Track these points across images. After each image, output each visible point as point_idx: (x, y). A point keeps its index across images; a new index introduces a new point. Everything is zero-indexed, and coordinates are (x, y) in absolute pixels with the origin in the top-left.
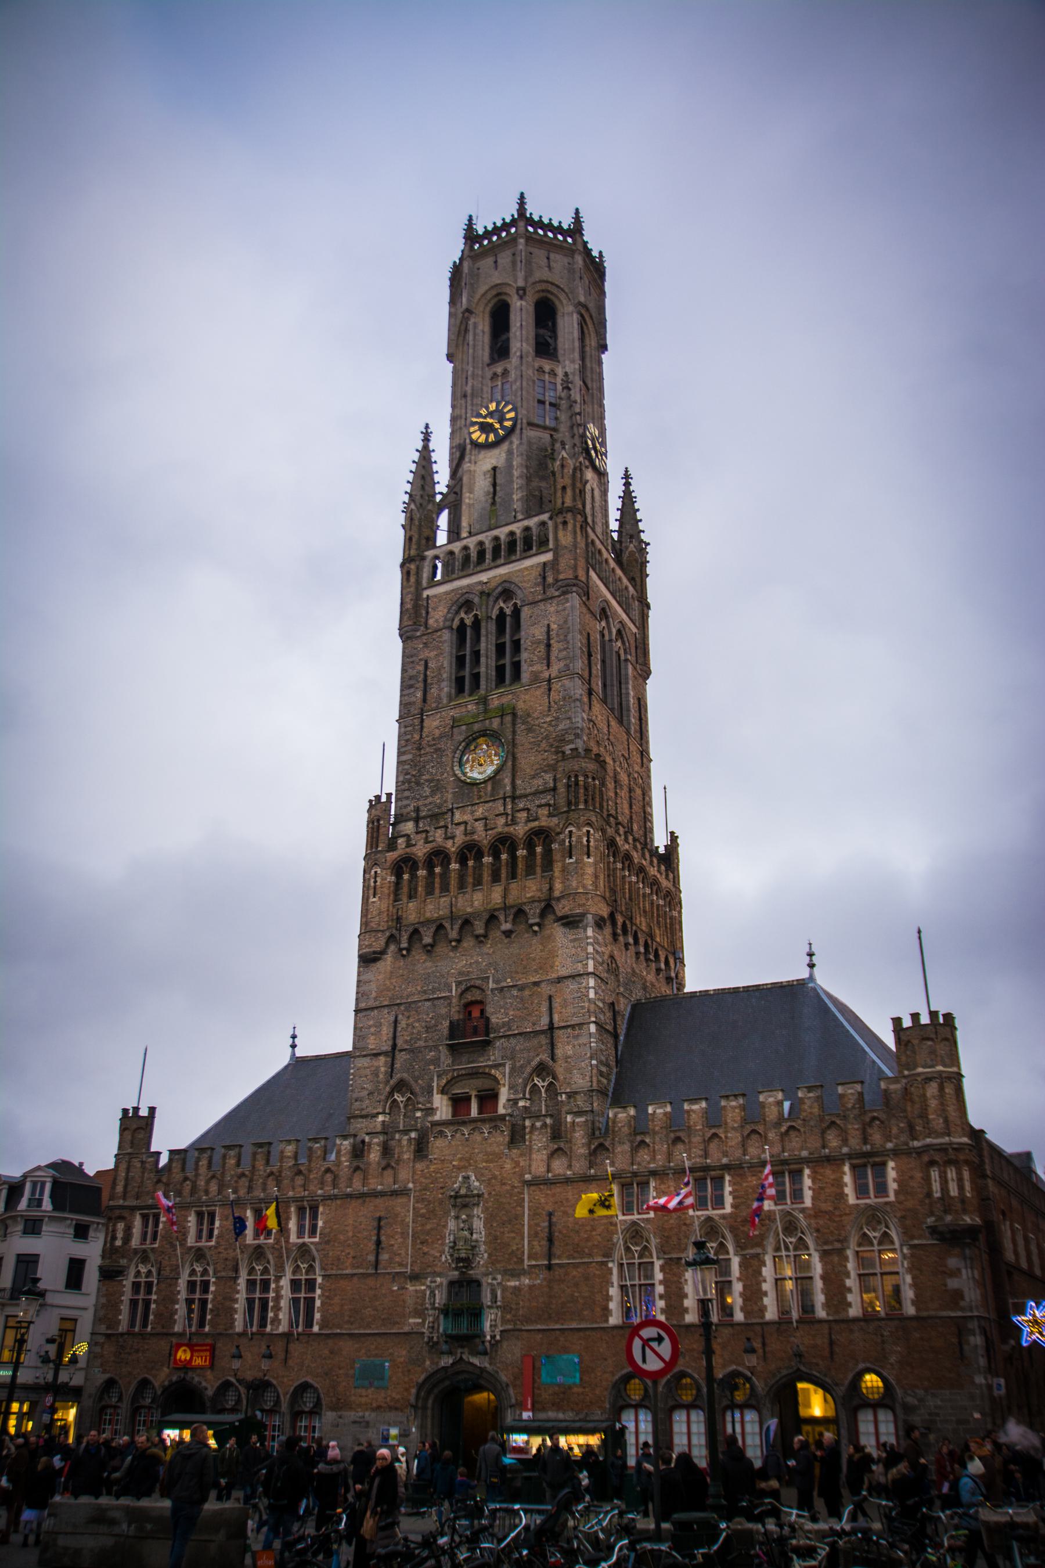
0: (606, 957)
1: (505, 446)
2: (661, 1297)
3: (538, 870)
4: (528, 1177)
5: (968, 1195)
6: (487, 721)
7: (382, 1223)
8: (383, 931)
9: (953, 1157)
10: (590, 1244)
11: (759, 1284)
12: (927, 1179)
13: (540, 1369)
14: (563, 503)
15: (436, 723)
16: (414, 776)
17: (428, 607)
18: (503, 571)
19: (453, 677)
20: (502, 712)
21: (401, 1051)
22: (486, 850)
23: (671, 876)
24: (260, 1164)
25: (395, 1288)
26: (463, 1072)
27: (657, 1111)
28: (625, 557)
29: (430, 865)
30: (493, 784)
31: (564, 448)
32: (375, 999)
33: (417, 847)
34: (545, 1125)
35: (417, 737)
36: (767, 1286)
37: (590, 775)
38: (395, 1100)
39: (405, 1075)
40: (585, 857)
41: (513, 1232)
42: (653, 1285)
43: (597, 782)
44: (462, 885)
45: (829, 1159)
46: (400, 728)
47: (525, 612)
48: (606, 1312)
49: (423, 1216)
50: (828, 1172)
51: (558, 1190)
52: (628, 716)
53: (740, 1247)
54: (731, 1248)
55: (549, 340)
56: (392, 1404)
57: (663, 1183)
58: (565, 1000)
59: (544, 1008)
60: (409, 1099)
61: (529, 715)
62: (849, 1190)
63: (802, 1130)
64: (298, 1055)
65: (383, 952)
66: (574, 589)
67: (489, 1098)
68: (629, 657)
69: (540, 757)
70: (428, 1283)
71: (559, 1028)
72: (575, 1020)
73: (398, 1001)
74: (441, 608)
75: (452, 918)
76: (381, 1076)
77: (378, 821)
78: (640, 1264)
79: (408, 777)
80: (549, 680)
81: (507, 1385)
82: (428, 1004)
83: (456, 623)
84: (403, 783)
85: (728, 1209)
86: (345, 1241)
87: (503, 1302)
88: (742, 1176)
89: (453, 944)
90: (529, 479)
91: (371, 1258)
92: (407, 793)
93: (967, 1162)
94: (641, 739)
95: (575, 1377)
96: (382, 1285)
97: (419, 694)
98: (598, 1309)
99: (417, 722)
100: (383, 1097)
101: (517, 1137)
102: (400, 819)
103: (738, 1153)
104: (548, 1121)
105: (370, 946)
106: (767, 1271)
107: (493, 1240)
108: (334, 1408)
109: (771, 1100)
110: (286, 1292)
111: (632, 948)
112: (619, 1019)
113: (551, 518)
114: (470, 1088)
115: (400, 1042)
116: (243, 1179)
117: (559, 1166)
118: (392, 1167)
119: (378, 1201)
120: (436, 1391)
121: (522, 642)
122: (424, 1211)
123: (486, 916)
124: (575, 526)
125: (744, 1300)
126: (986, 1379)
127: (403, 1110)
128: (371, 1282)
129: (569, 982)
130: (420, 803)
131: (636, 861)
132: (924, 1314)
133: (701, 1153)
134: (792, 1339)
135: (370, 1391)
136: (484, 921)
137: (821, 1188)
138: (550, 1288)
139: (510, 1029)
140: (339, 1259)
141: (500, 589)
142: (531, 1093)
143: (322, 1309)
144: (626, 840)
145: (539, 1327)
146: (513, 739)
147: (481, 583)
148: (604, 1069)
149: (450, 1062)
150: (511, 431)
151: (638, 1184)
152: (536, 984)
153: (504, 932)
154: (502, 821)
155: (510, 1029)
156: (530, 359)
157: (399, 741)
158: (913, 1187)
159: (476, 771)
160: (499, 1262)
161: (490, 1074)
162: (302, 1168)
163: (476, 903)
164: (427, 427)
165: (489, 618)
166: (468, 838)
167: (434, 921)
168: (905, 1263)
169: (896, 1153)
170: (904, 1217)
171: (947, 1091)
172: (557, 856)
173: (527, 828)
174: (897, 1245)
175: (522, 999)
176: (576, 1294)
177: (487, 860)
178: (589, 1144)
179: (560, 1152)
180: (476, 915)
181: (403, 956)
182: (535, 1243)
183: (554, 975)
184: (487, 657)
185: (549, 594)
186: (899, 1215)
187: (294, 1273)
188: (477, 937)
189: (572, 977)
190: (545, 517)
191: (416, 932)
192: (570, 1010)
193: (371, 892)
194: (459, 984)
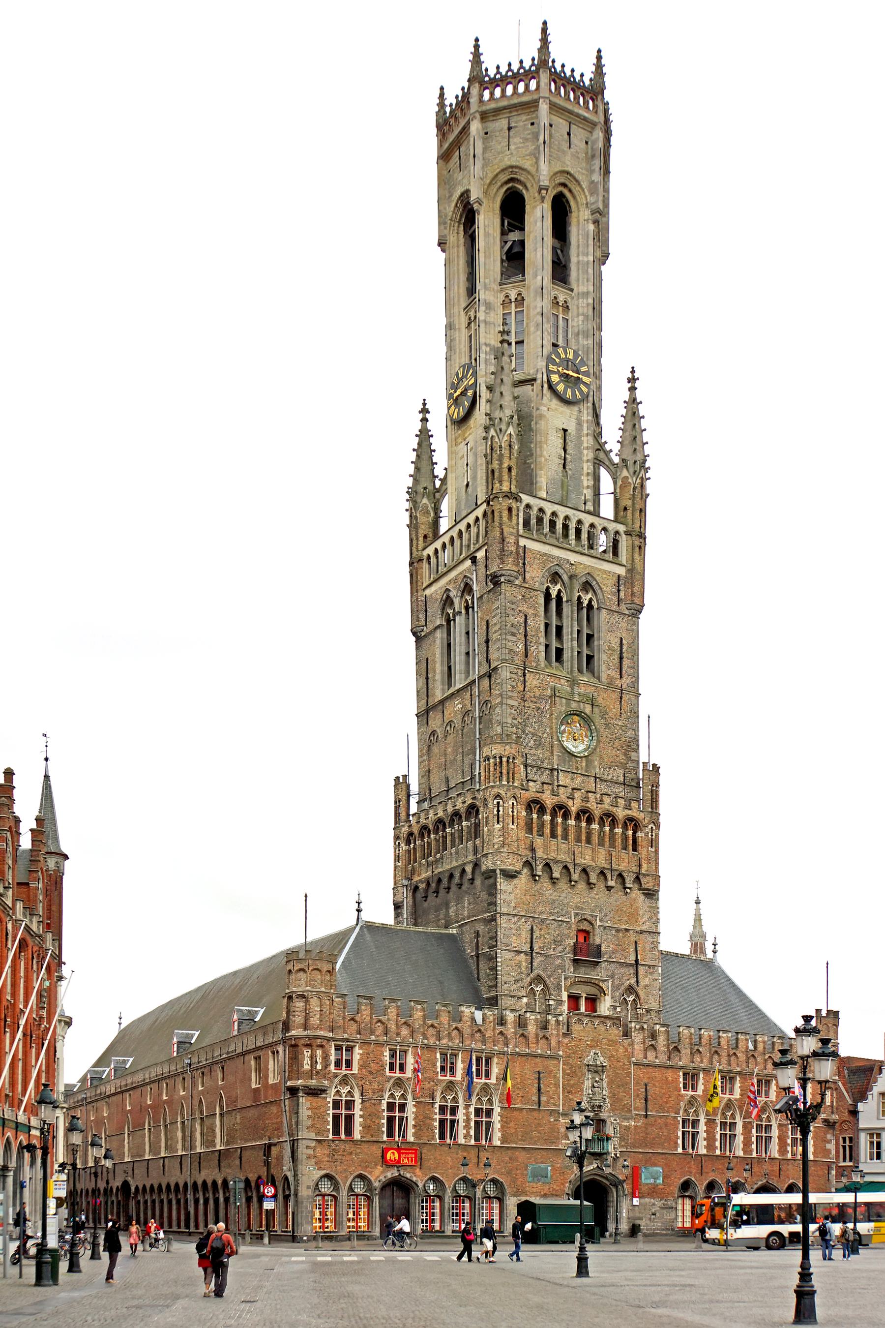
3: (630, 847)
7: (541, 1075)
8: (520, 855)
11: (751, 1137)
15: (536, 682)
24: (444, 1019)
29: (554, 815)
39: (541, 973)
44: (578, 840)
51: (650, 1070)
56: (554, 1192)
59: (632, 948)
60: (542, 989)
65: (519, 873)
67: (592, 1002)
73: (532, 915)
76: (523, 969)
77: (514, 758)
88: (745, 1079)
89: (573, 883)
91: (535, 1098)
97: (521, 647)
99: (520, 673)
100: (525, 985)
103: (744, 1065)
107: (613, 1096)
109: (761, 1039)
110: (472, 1116)
114: (583, 992)
115: (535, 947)
116: (431, 1029)
118: (547, 1039)
119: (538, 1060)
128: (535, 1114)
129: (647, 935)
132: (817, 1159)
133: (726, 1062)
138: (646, 1128)
143: (503, 1129)
145: (640, 1151)
152: (627, 930)
155: (610, 957)
160: (617, 1110)
161: (598, 985)
163: (587, 857)
166: (584, 804)
167: (562, 862)
175: (618, 937)
177: (595, 826)
181: (535, 880)
182: (637, 1101)
189: (650, 932)
194: (576, 915)
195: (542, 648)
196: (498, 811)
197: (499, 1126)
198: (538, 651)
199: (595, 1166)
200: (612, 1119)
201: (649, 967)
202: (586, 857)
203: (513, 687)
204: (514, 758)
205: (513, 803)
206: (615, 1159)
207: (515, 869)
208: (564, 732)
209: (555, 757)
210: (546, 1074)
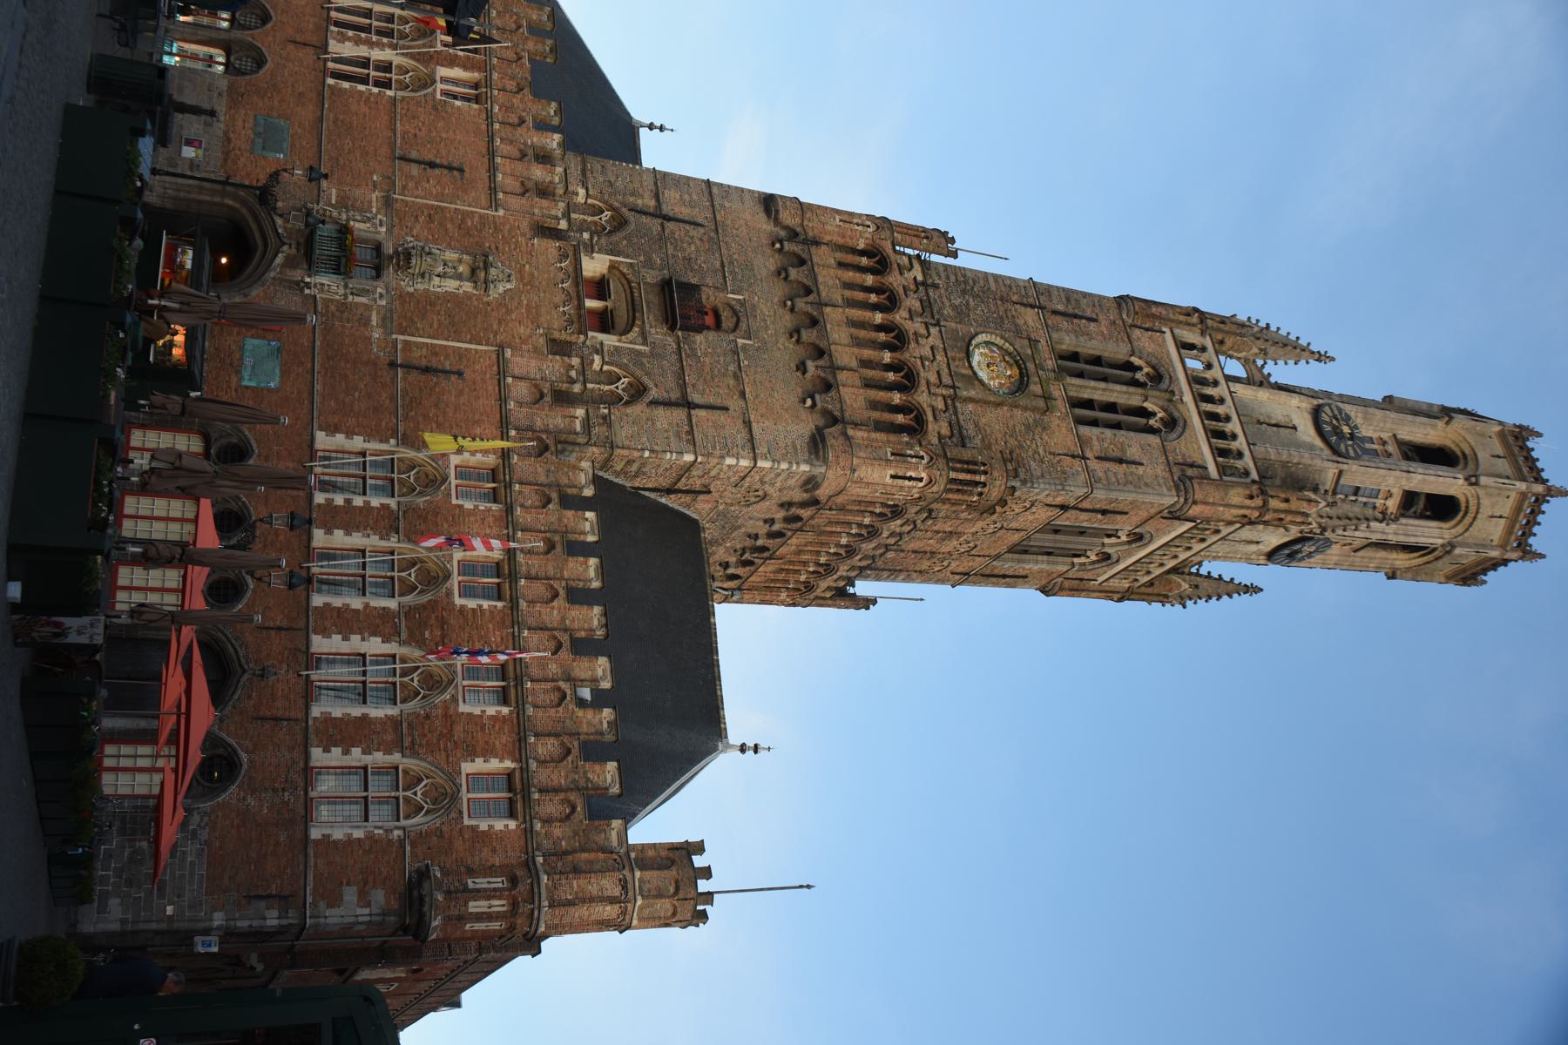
0: (767, 488)
1: (1318, 442)
2: (348, 501)
4: (508, 353)
5: (468, 927)
6: (1037, 379)
7: (455, 173)
9: (521, 911)
10: (420, 418)
12: (490, 871)
13: (264, 338)
14: (1272, 497)
15: (1030, 322)
16: (973, 288)
17: (1153, 330)
18: (1196, 420)
19: (1079, 350)
20: (1047, 397)
21: (662, 225)
22: (897, 355)
23: (828, 595)
24: (530, 45)
25: (375, 178)
26: (636, 294)
28: (1174, 577)
30: (968, 376)
31: (1328, 505)
32: (723, 206)
33: (899, 277)
34: (572, 382)
35: (1015, 298)
36: (356, 643)
37: (986, 490)
38: (603, 212)
39: (633, 227)
40: (892, 472)
41: (440, 325)
42: (364, 493)
43: (975, 498)
45: (521, 740)
46: (1024, 281)
47: (1154, 440)
48: (332, 430)
49: (463, 221)
50: (504, 739)
51: (490, 388)
52: (1013, 560)
53: (409, 612)
54: (408, 599)
55: (1413, 510)
56: (232, 156)
57: (496, 519)
58: (723, 427)
59: (712, 400)
61: (1044, 429)
62: (477, 765)
63: (560, 709)
64: (641, 129)
65: (777, 222)
66: (1182, 500)
67: (604, 322)
68: (1076, 568)
69: (999, 436)
70: (379, 217)
71: (689, 417)
72: (698, 436)
74: (1152, 345)
75: (821, 304)
76: (631, 199)
77: (927, 238)
78: (392, 480)
79: (971, 282)
80: (1084, 458)
81: (246, 296)
82: (718, 264)
83: (1135, 360)
84: (964, 276)
85: (458, 601)
86: (436, 129)
87: (351, 303)
89: (789, 303)
90: (1285, 464)
91: (414, 155)
92: (953, 278)
93: (512, 928)
94: (982, 575)
95: (250, 380)
96: (380, 163)
97: (1060, 307)
98: (336, 420)
99: (1031, 300)
100: (606, 197)
101: (560, 348)
102: (925, 265)
103: (531, 621)
104: (577, 388)
105: (785, 207)
106: (375, 646)
107: (430, 301)
108: (231, 87)
110: (377, 55)
111: (780, 515)
112: (687, 499)
113: (1254, 482)
115: (670, 226)
116: (514, 26)
117: (520, 390)
118: (523, 194)
119: (485, 175)
120: (244, 211)
121: (1123, 432)
122: (469, 224)
123: (823, 344)
124: (1248, 508)
125: (339, 609)
126: (219, 928)
127: (590, 219)
128: (384, 150)
129: (744, 434)
130: (942, 291)
131: (864, 545)
132: (311, 852)
133: (533, 572)
134: (285, 667)
135: (250, 132)
136: (818, 342)
137: (483, 728)
139: (688, 356)
140: (414, 118)
141: (1176, 414)
142: (610, 372)
143: (352, 92)
144: (892, 534)
145: (318, 343)
146: (1016, 407)
147: (1181, 393)
148: (634, 468)
149: (649, 280)
150: (1335, 452)
151: (494, 489)
152: (743, 394)
153: (803, 363)
154: (933, 378)
156: (1404, 483)
157: (1010, 278)
158: (480, 851)
159: (982, 360)
161: (633, 325)
162: (526, 91)
164: (1333, 359)
165: (1146, 400)
166: (911, 336)
168: (381, 832)
169: (528, 832)
170: (441, 836)
171: (608, 908)
172: (893, 437)
173: (925, 406)
174: (403, 822)
175: (725, 375)
176: (357, 394)
177: (887, 357)
178: (547, 431)
179: (538, 396)
180: (824, 333)
181: (773, 244)
183: (752, 417)
184: (1104, 390)
185: (1175, 469)
186: (444, 828)
187: (399, 67)
188: (798, 332)
189: (751, 439)
190: (1254, 475)
191: (802, 262)
192: (712, 432)
193: (846, 218)
194: (742, 303)
199: (286, 241)
200: (384, 292)
202: (838, 335)
205: (869, 226)
206: (299, 286)
207: (781, 209)
210: (459, 183)
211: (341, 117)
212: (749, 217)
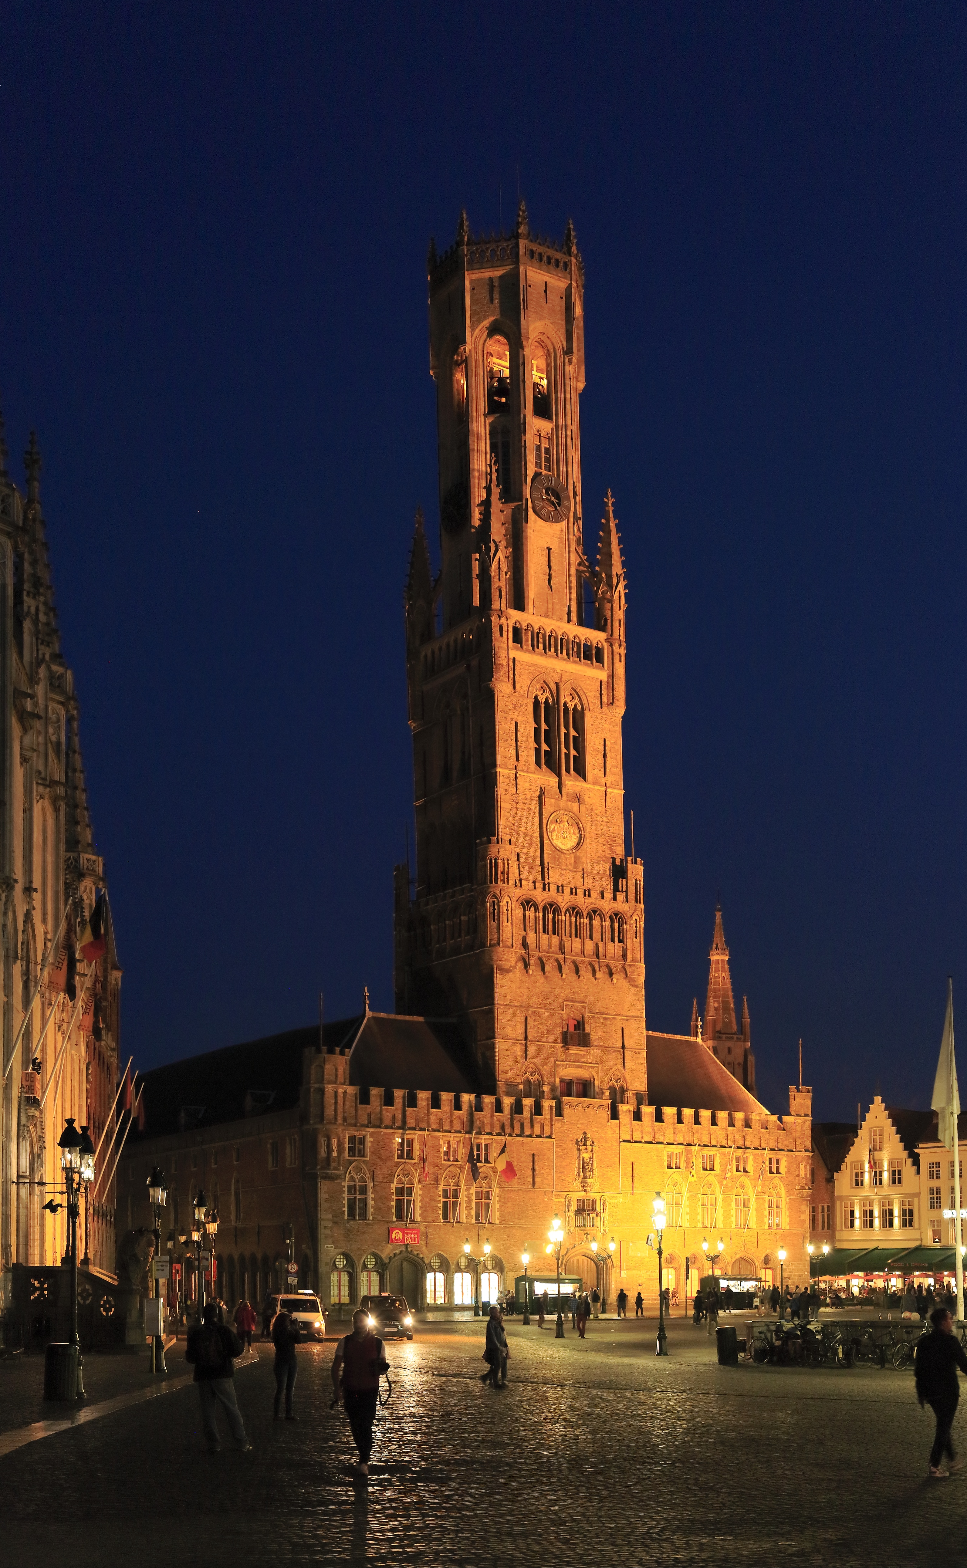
6: (570, 803)
7: (536, 1158)
15: (527, 785)
27: (688, 1112)
30: (575, 858)
39: (535, 1060)
76: (519, 1058)
79: (509, 824)
84: (506, 827)
97: (513, 752)
110: (473, 1197)
115: (529, 1037)
147: (554, 670)
175: (606, 1025)
182: (625, 1179)
195: (533, 752)
196: (494, 909)
197: (497, 1206)
198: (528, 755)
201: (635, 1052)
203: (506, 790)
204: (508, 860)
205: (507, 903)
208: (554, 830)
209: (546, 856)
211: (517, 1216)
212: (514, 986)
